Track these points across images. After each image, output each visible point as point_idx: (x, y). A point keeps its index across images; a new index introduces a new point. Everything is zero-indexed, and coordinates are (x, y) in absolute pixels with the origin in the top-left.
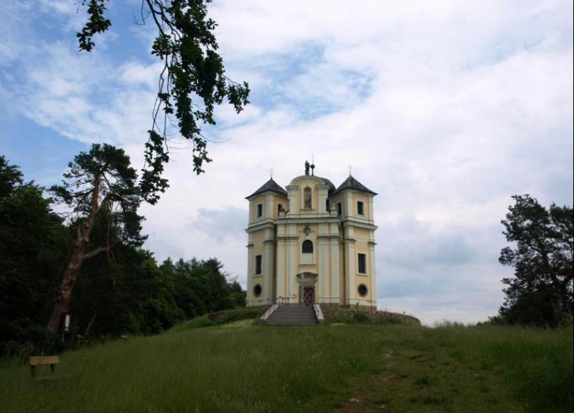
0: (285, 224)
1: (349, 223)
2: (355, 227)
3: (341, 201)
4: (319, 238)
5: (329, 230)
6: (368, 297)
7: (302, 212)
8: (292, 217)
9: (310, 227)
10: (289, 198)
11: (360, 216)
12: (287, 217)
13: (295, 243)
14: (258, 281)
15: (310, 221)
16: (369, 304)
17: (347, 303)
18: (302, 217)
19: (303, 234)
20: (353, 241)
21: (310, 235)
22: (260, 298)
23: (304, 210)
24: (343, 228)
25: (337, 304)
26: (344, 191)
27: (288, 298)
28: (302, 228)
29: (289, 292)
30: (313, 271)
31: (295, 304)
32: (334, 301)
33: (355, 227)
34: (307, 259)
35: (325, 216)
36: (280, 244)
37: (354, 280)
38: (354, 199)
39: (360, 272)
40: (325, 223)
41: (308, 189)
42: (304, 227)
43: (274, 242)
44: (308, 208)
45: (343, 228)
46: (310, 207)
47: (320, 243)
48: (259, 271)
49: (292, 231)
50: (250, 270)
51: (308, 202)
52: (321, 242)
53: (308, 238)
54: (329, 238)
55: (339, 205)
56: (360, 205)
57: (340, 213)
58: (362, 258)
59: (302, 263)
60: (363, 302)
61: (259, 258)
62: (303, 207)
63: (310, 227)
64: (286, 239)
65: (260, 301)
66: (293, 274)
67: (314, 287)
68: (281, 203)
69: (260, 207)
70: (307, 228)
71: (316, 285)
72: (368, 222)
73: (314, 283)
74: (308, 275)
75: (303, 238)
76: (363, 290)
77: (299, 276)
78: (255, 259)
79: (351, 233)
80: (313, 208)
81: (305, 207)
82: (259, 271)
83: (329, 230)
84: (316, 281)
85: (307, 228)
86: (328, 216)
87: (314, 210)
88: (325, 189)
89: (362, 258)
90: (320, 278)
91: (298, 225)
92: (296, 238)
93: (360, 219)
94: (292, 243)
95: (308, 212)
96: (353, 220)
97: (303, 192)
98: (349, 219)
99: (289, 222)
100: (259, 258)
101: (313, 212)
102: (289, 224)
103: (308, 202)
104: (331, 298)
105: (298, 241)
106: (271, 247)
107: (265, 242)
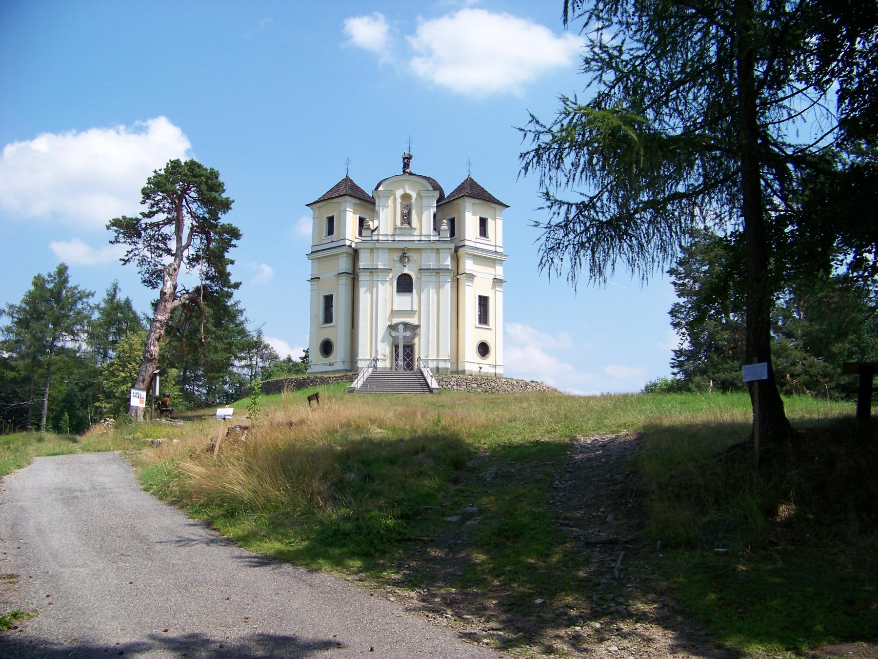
0: (372, 249)
3: (455, 216)
5: (438, 260)
6: (490, 358)
7: (398, 232)
8: (381, 238)
10: (377, 208)
11: (483, 240)
12: (375, 238)
14: (328, 333)
16: (492, 371)
17: (460, 369)
18: (397, 238)
19: (398, 265)
20: (471, 277)
22: (330, 359)
24: (456, 259)
25: (446, 369)
26: (456, 202)
28: (397, 256)
29: (377, 351)
30: (414, 321)
31: (385, 368)
34: (403, 302)
35: (432, 238)
36: (363, 278)
37: (472, 335)
38: (474, 214)
39: (480, 322)
40: (433, 249)
41: (406, 197)
42: (399, 254)
43: (353, 276)
44: (406, 226)
45: (456, 259)
46: (409, 223)
51: (407, 218)
52: (425, 277)
54: (438, 271)
55: (452, 222)
56: (483, 222)
57: (452, 234)
58: (483, 302)
59: (396, 308)
60: (486, 366)
62: (399, 224)
64: (372, 271)
65: (331, 365)
66: (383, 325)
68: (363, 216)
69: (331, 220)
70: (404, 256)
71: (416, 340)
72: (493, 249)
73: (413, 338)
75: (400, 270)
76: (484, 349)
77: (393, 327)
79: (469, 265)
81: (402, 224)
83: (438, 260)
85: (404, 256)
86: (437, 238)
87: (415, 229)
88: (432, 197)
89: (483, 302)
90: (423, 330)
93: (483, 244)
96: (473, 245)
97: (399, 200)
98: (467, 243)
99: (378, 245)
103: (407, 218)
104: (438, 360)
106: (350, 282)
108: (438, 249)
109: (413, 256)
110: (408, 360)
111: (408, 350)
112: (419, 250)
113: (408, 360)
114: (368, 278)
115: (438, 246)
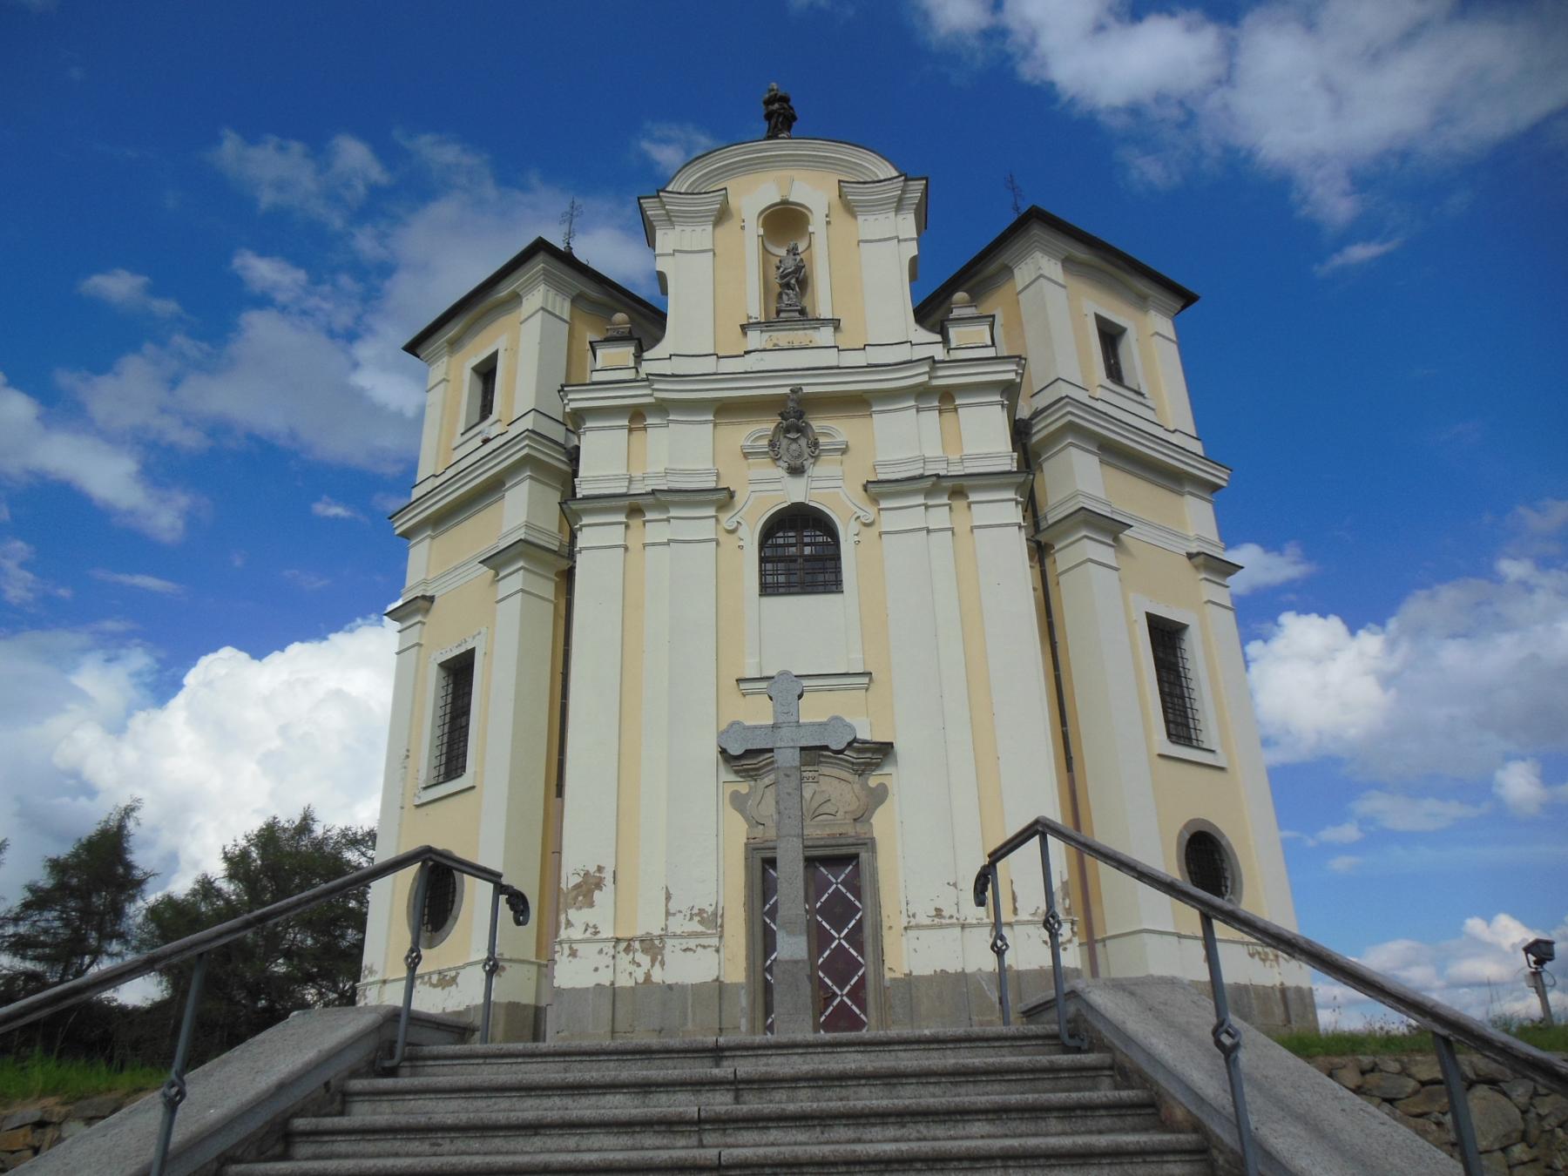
4: (877, 490)
7: (755, 339)
9: (818, 423)
13: (706, 529)
21: (815, 470)
23: (766, 325)
27: (652, 946)
36: (595, 535)
42: (768, 425)
47: (889, 521)
48: (452, 758)
50: (400, 758)
54: (955, 488)
61: (459, 671)
63: (818, 423)
64: (634, 507)
67: (870, 844)
71: (881, 824)
73: (862, 817)
78: (432, 684)
82: (452, 758)
84: (879, 796)
87: (836, 324)
88: (899, 206)
91: (726, 409)
92: (722, 498)
95: (783, 337)
97: (754, 229)
100: (459, 671)
101: (825, 335)
105: (727, 520)
106: (547, 588)
107: (496, 561)
110: (839, 938)
111: (836, 881)
112: (857, 403)
113: (839, 938)
114: (616, 535)
115: (946, 379)
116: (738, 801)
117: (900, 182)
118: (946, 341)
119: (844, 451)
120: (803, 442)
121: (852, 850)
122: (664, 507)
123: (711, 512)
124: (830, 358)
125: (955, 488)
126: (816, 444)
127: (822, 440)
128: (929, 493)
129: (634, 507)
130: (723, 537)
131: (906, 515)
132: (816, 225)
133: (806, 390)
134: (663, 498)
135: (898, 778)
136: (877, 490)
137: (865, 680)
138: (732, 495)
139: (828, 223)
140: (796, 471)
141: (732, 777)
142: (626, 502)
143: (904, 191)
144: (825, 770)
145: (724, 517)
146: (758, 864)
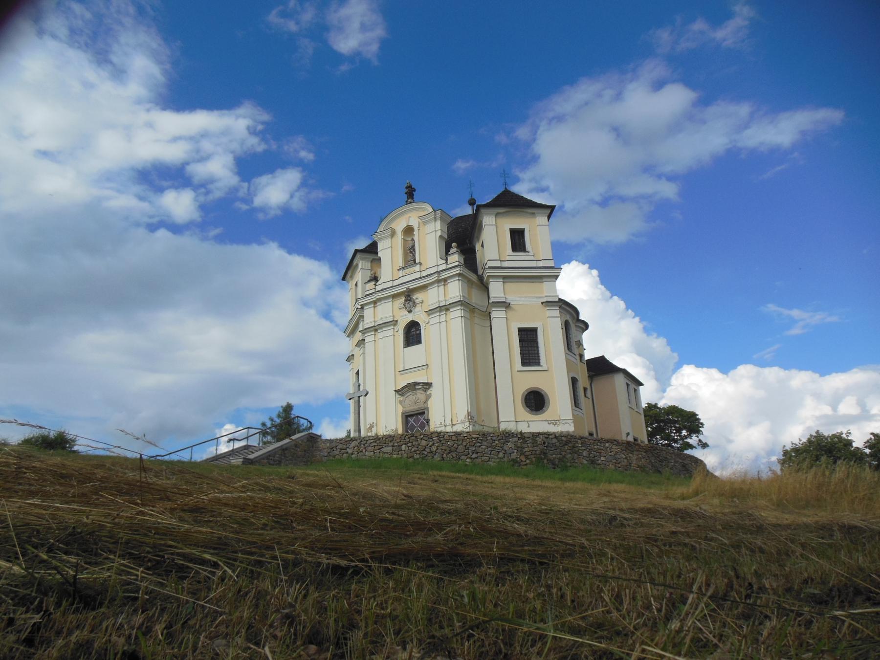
0: (375, 302)
1: (489, 272)
2: (505, 278)
4: (430, 312)
6: (547, 414)
7: (401, 273)
12: (379, 288)
13: (391, 332)
15: (412, 286)
23: (403, 268)
32: (459, 428)
33: (505, 278)
42: (403, 300)
46: (415, 260)
47: (432, 321)
49: (386, 311)
53: (409, 318)
54: (444, 308)
64: (375, 329)
70: (408, 297)
73: (426, 402)
74: (412, 387)
75: (405, 318)
80: (417, 261)
84: (429, 397)
85: (408, 297)
86: (444, 267)
91: (394, 297)
92: (395, 323)
94: (388, 332)
95: (407, 271)
101: (417, 268)
102: (380, 300)
105: (396, 328)
108: (445, 280)
109: (418, 297)
112: (424, 287)
115: (444, 275)
116: (401, 402)
117: (433, 213)
118: (447, 262)
119: (422, 303)
120: (411, 303)
121: (423, 411)
122: (381, 328)
123: (392, 327)
124: (417, 275)
125: (444, 308)
126: (414, 303)
127: (416, 301)
128: (440, 311)
129: (375, 329)
130: (396, 334)
131: (435, 318)
132: (416, 233)
133: (410, 288)
134: (380, 326)
135: (433, 391)
136: (430, 312)
137: (426, 367)
138: (397, 321)
139: (419, 230)
140: (410, 312)
141: (399, 396)
142: (372, 329)
143: (435, 215)
144: (418, 391)
145: (395, 328)
146: (404, 417)
